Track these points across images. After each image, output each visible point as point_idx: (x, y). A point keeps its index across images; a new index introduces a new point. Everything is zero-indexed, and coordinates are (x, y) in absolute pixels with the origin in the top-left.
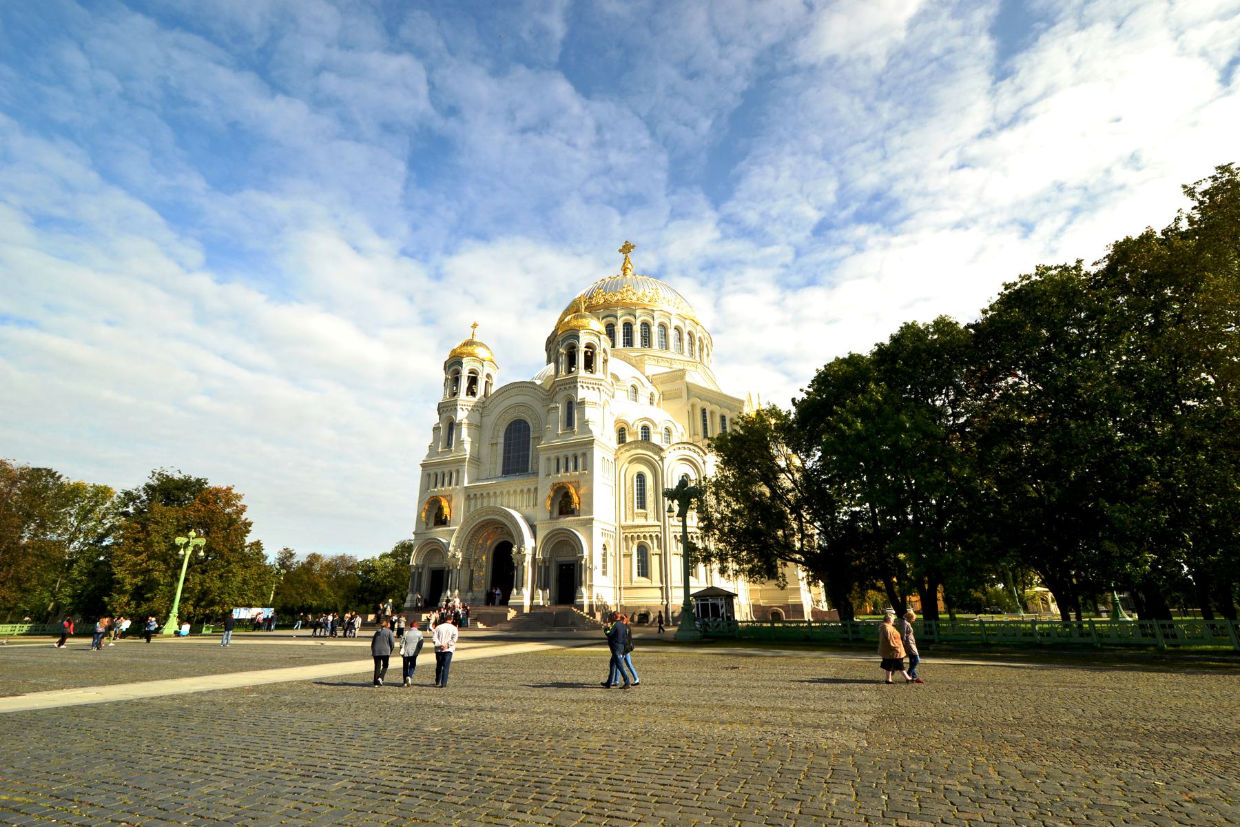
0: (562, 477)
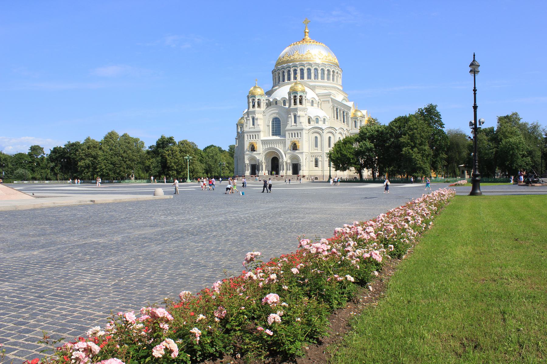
0: (295, 139)
